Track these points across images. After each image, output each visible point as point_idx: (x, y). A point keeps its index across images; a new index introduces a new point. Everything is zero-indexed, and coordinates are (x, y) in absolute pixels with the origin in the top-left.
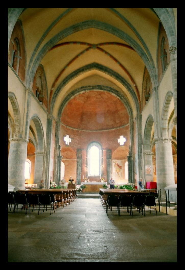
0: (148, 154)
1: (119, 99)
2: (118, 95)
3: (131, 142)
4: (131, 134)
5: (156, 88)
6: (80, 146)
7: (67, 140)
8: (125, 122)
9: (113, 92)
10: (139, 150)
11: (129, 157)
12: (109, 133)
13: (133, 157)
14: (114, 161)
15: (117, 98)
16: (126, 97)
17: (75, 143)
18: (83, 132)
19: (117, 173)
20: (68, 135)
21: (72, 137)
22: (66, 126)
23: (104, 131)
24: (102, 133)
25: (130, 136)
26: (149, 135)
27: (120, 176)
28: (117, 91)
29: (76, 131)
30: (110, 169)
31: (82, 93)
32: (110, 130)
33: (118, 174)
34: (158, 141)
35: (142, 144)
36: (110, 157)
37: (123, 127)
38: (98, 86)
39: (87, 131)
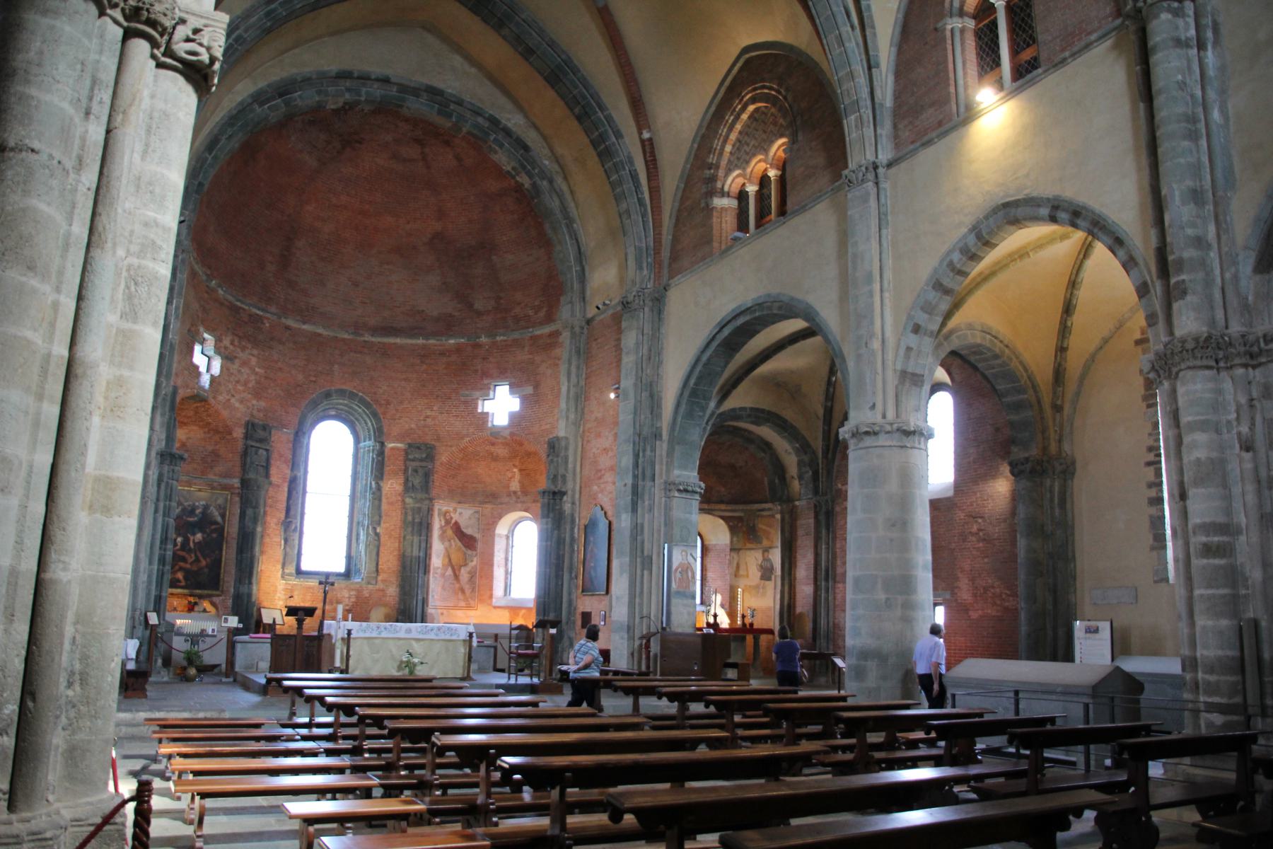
0: (686, 491)
1: (519, 187)
2: (524, 167)
3: (567, 418)
4: (569, 381)
5: (881, 171)
6: (262, 404)
7: (206, 361)
8: (531, 313)
9: (501, 146)
10: (636, 465)
11: (554, 493)
12: (425, 355)
13: (573, 496)
14: (440, 506)
15: (513, 177)
16: (565, 188)
17: (240, 387)
18: (288, 328)
19: (449, 572)
20: (210, 330)
21: (226, 348)
22: (204, 278)
23: (398, 340)
24: (385, 351)
25: (564, 389)
26: (704, 398)
27: (467, 587)
28: (526, 148)
29: (255, 320)
30: (423, 545)
31: (333, 107)
32: (432, 341)
33: (456, 577)
34: (876, 434)
35: (657, 436)
36: (427, 482)
37: (516, 335)
38: (433, 92)
39: (305, 327)
